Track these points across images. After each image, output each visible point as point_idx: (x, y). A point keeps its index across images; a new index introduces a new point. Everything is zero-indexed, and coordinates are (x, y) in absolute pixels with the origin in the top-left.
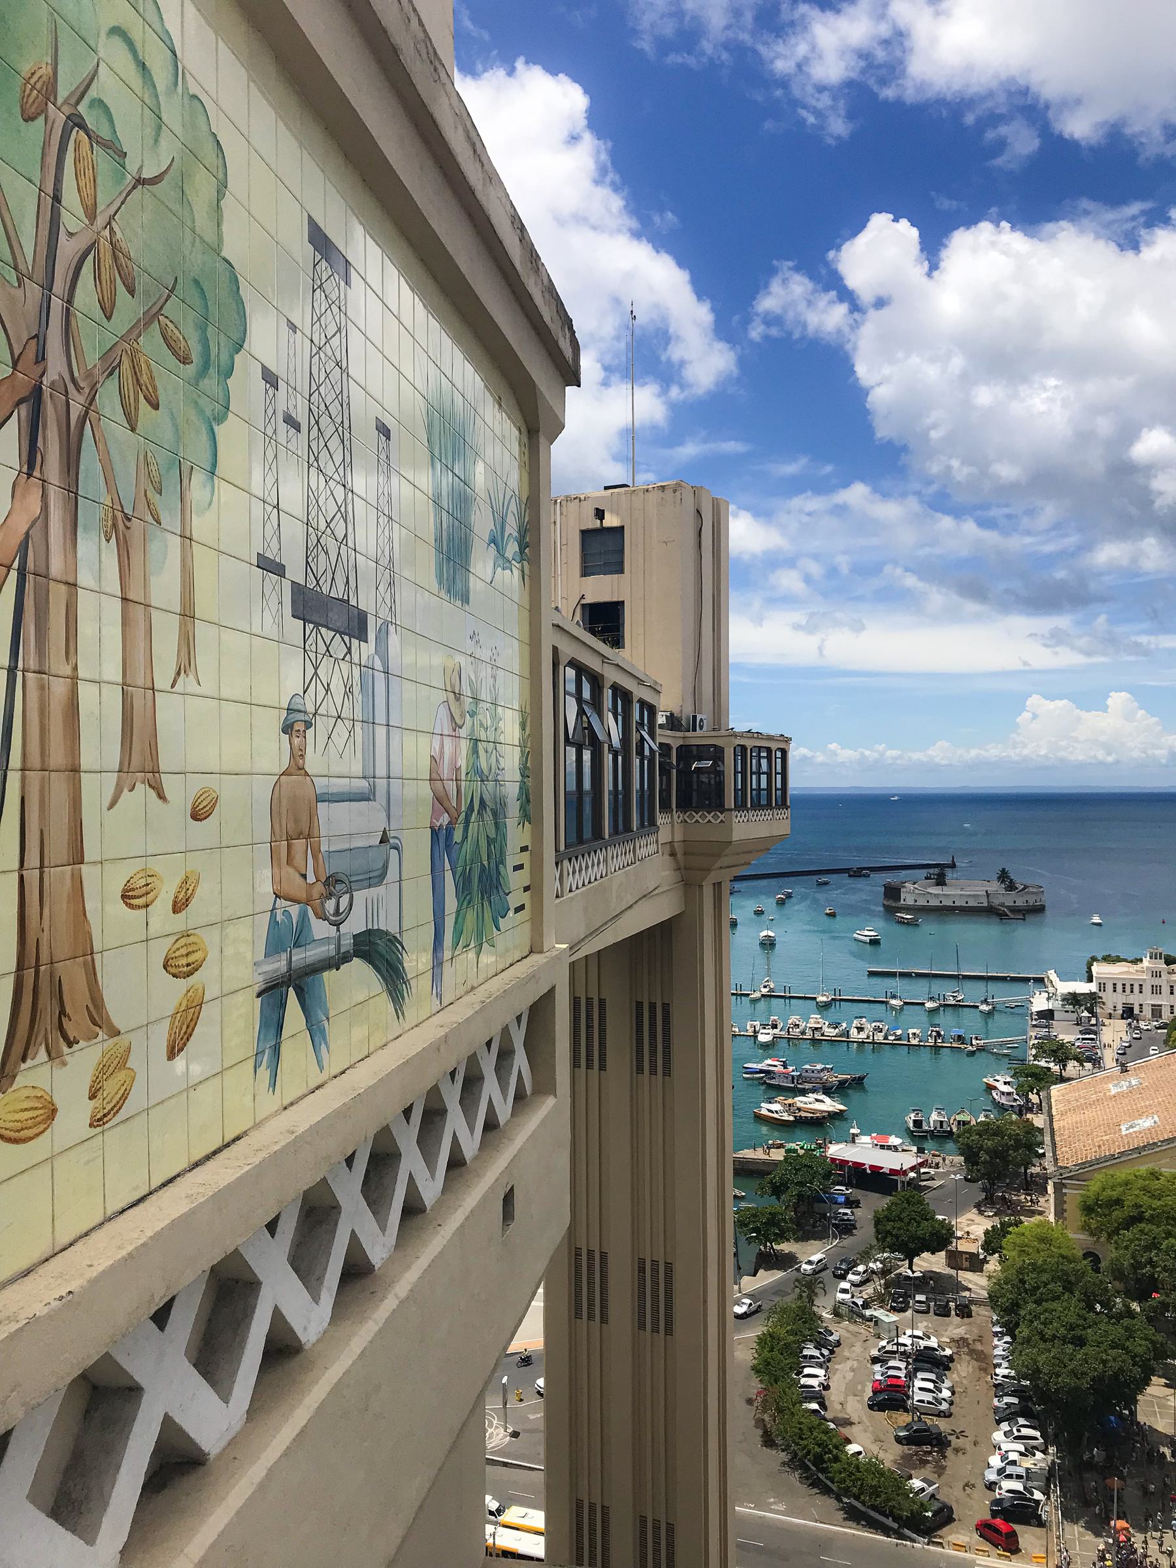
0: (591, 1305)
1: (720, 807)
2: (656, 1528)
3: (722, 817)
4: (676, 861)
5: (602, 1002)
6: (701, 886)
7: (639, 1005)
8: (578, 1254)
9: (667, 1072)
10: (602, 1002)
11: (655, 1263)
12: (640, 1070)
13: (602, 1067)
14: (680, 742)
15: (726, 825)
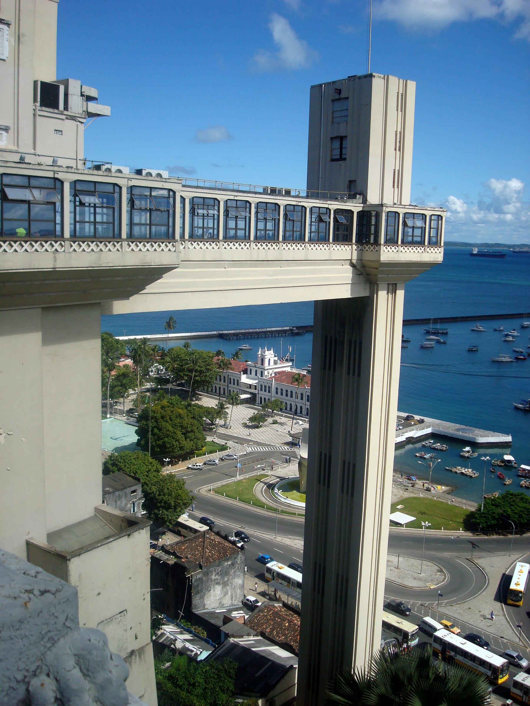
0: (324, 479)
1: (377, 242)
2: (342, 579)
3: (377, 248)
4: (357, 269)
5: (336, 338)
6: (378, 284)
7: (350, 342)
8: (321, 455)
9: (359, 375)
10: (336, 338)
11: (349, 463)
12: (349, 373)
13: (334, 371)
14: (361, 209)
15: (379, 251)
